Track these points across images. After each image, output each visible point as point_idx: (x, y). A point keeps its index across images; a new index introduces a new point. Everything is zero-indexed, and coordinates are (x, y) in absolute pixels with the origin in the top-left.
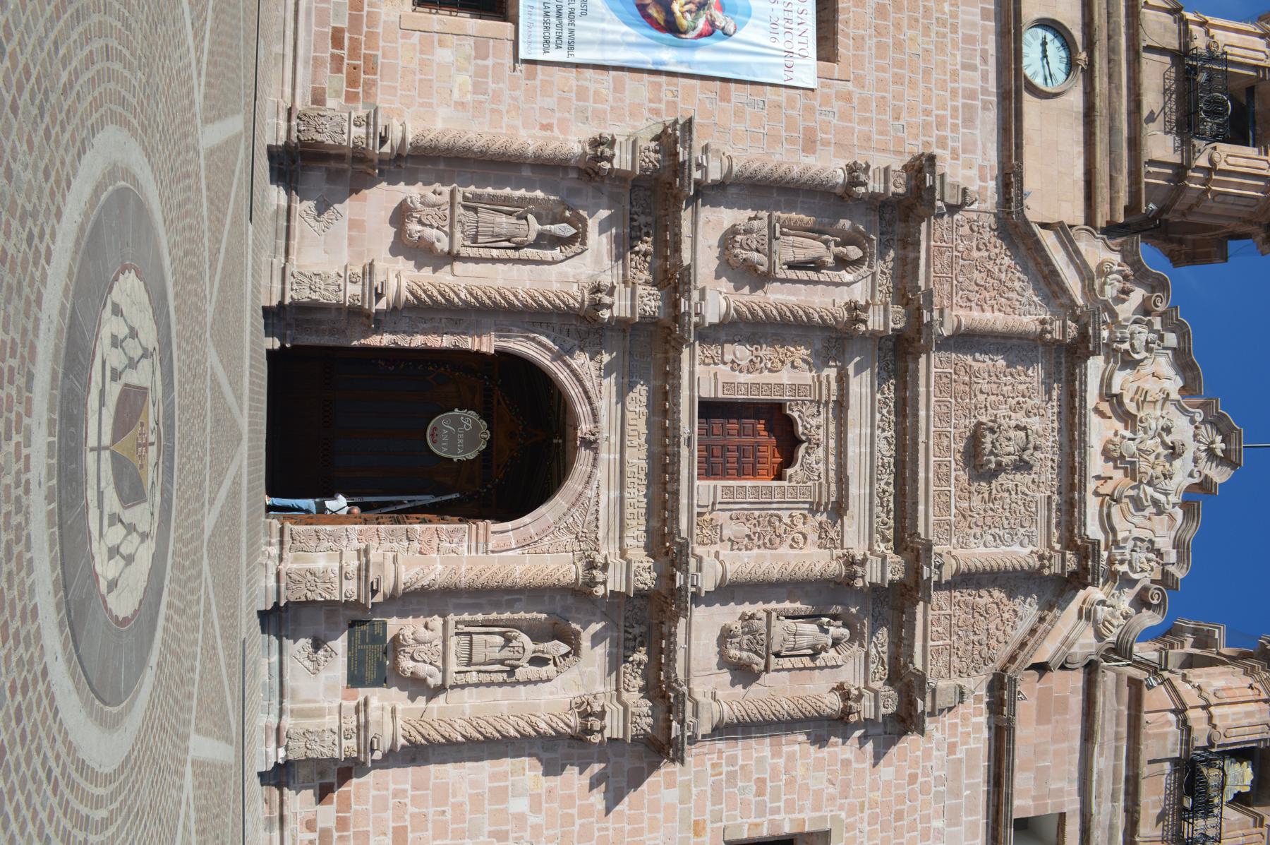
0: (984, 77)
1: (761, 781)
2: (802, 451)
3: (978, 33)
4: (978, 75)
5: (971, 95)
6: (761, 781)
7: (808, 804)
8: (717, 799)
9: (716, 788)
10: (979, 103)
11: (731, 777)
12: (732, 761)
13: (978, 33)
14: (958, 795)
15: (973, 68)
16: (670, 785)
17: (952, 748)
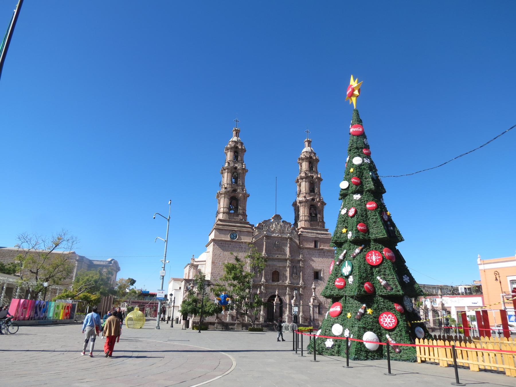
0: (237, 245)
1: (308, 276)
2: (277, 270)
3: (233, 246)
4: (237, 246)
5: (239, 247)
6: (308, 276)
7: (311, 271)
8: (309, 281)
9: (309, 281)
10: (240, 246)
11: (308, 279)
12: (306, 279)
13: (233, 246)
14: (311, 254)
15: (236, 247)
16: (308, 286)
17: (307, 254)
